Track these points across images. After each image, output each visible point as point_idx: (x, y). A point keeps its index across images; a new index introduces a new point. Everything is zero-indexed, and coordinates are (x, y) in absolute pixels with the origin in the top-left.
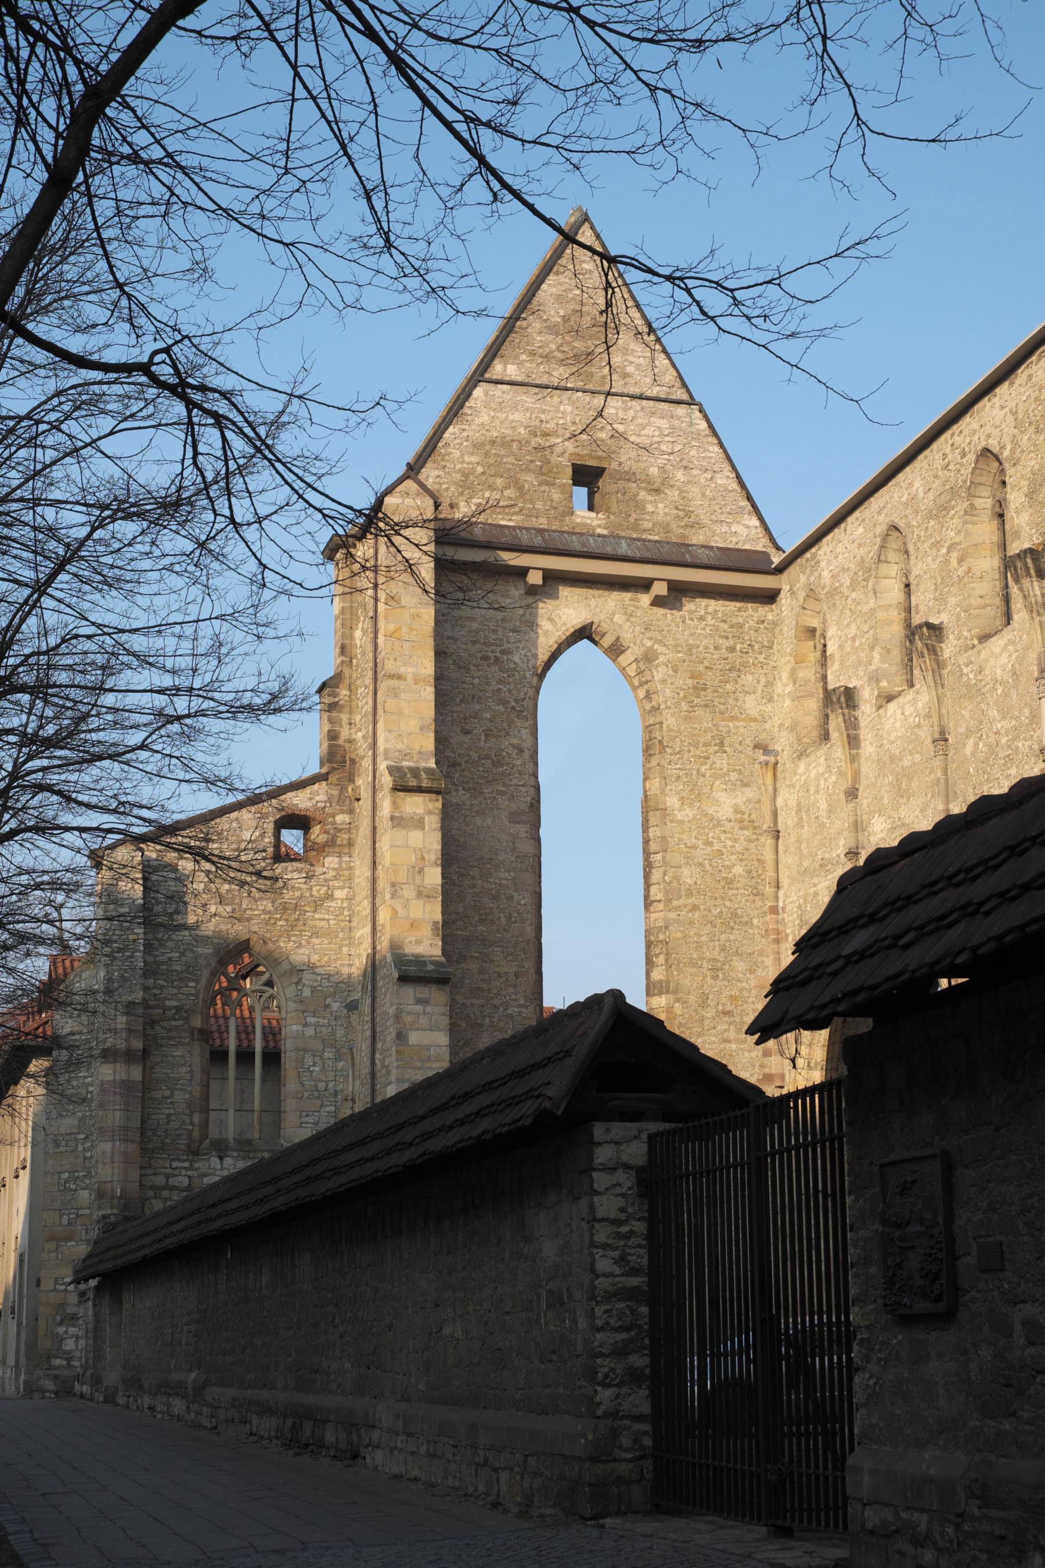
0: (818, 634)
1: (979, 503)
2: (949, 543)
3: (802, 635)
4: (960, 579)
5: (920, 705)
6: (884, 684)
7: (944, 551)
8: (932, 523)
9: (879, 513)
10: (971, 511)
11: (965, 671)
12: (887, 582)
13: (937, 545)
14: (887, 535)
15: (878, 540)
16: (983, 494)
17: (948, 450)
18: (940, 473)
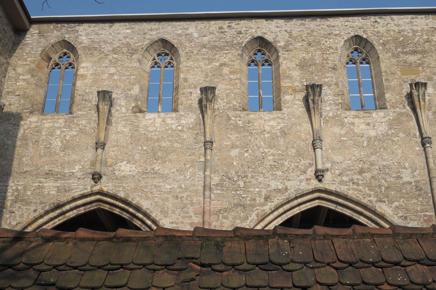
0: (52, 62)
1: (244, 55)
2: (222, 62)
3: (45, 58)
4: (231, 80)
5: (183, 122)
6: (139, 103)
7: (217, 64)
8: (205, 50)
9: (151, 30)
10: (241, 56)
11: (233, 118)
12: (146, 60)
13: (211, 60)
14: (156, 41)
15: (147, 42)
16: (247, 53)
17: (225, 27)
18: (215, 33)
